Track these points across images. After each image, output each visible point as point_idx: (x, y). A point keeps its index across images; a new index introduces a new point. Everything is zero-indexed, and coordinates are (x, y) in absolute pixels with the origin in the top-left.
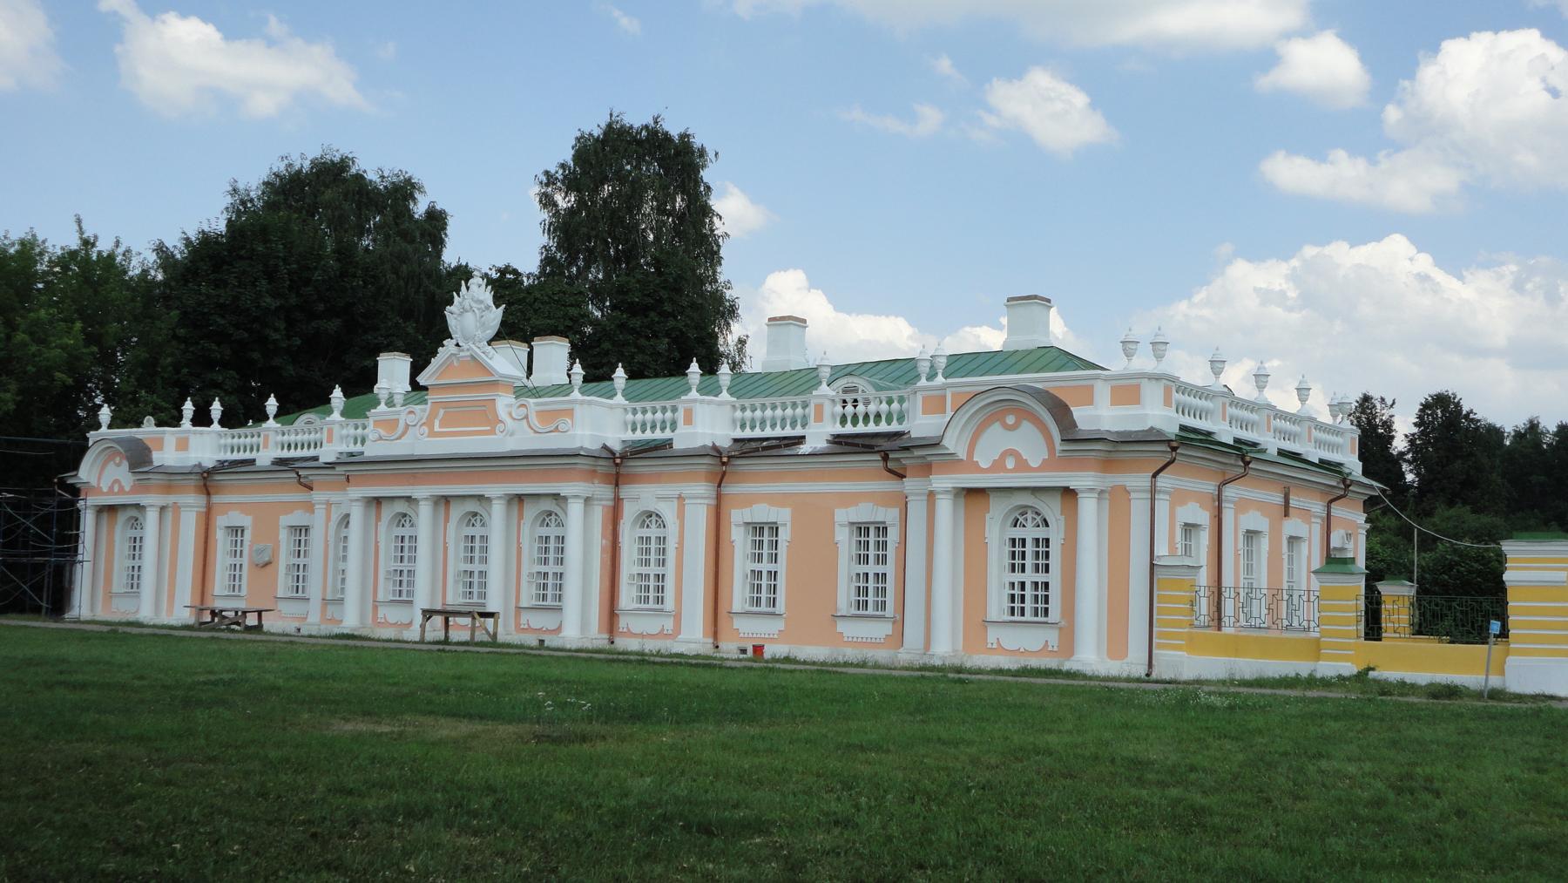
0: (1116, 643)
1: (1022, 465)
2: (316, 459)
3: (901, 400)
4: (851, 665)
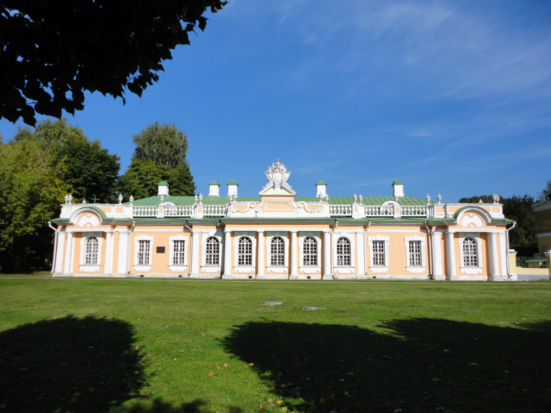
3: (155, 208)
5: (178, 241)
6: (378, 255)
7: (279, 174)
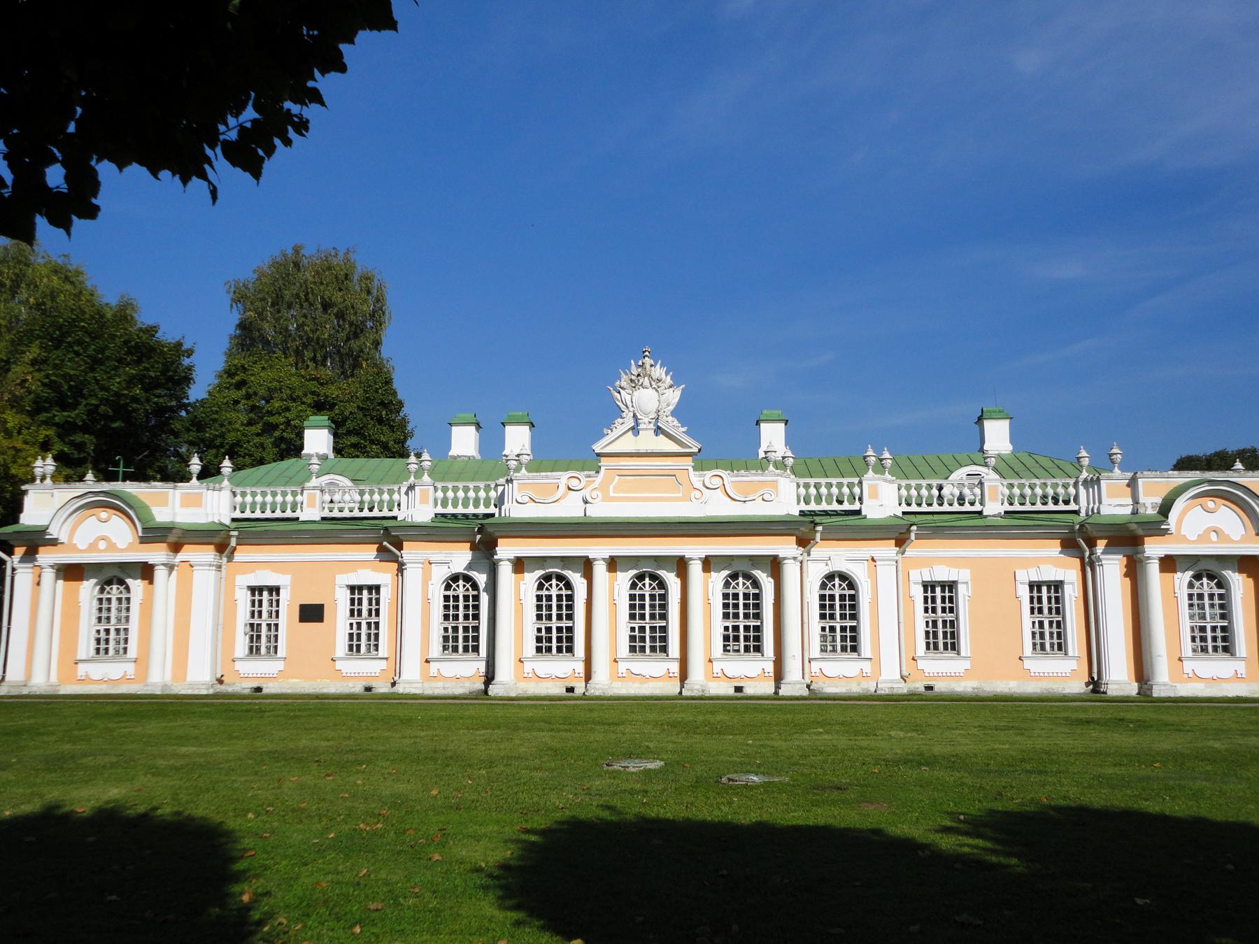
3: (294, 494)
5: (360, 588)
6: (940, 624)
7: (650, 391)
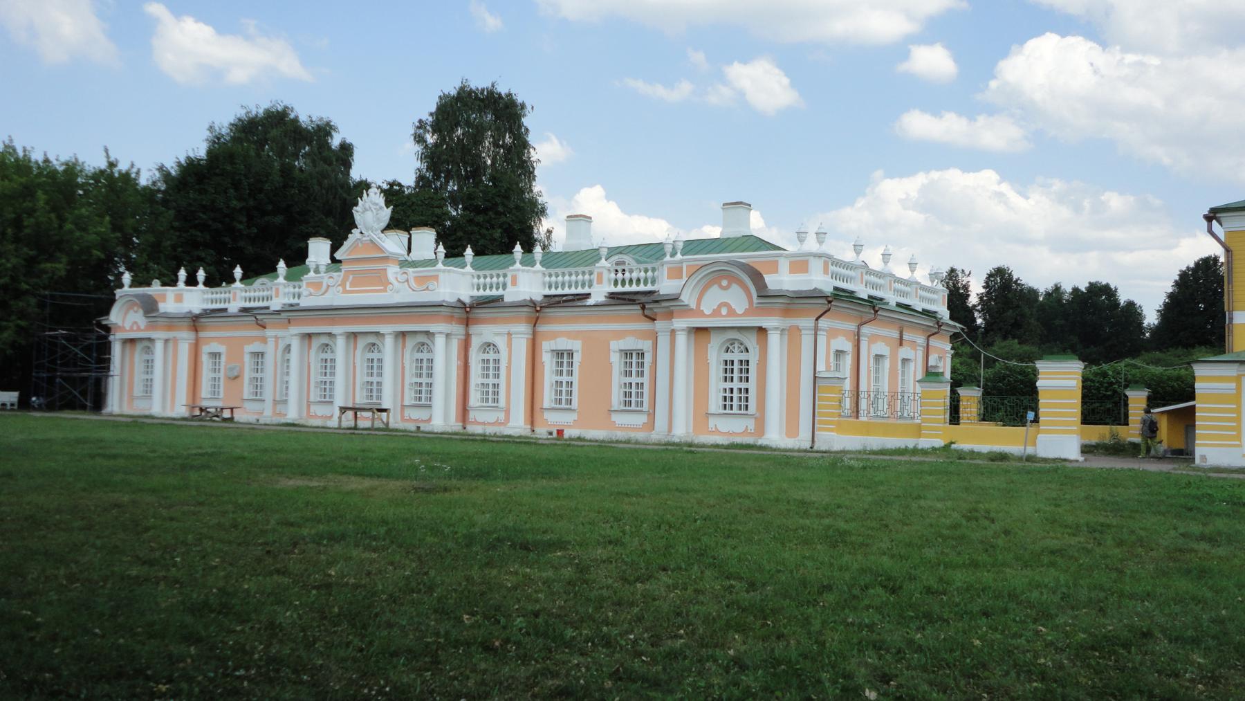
0: (791, 426)
1: (731, 312)
2: (268, 308)
3: (654, 270)
4: (621, 442)
